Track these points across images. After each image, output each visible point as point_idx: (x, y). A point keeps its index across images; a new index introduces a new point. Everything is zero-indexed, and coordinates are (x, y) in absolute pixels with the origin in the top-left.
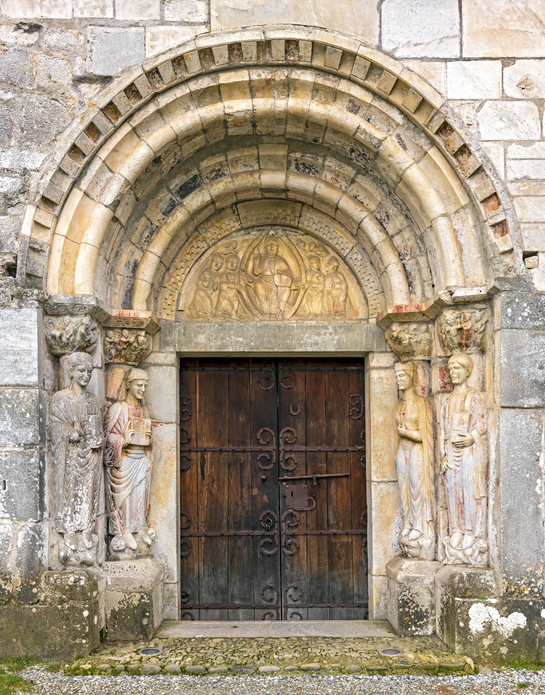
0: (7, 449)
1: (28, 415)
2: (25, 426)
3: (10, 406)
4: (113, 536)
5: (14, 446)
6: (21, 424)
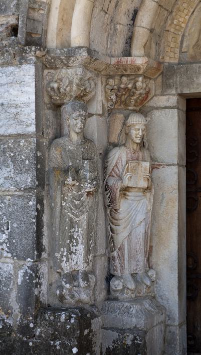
0: (11, 193)
1: (27, 162)
2: (25, 172)
3: (12, 154)
4: (113, 276)
5: (16, 191)
6: (21, 170)
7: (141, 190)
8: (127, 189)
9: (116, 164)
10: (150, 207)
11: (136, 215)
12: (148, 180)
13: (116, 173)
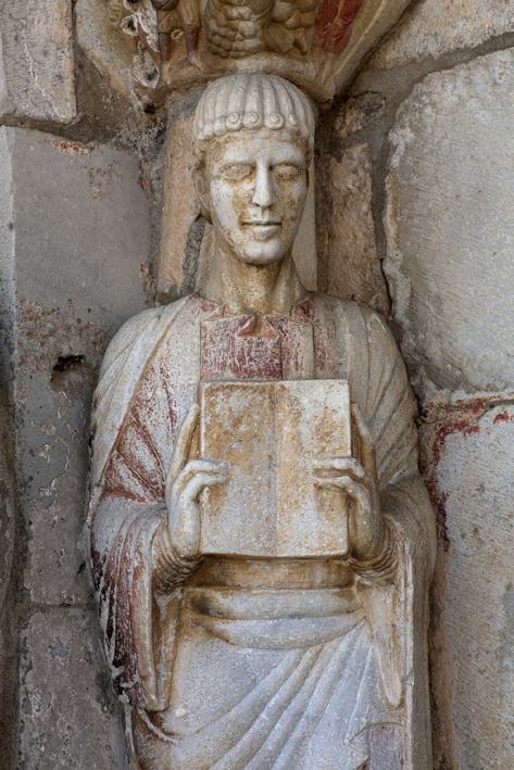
7: (320, 574)
8: (215, 571)
9: (133, 410)
10: (398, 685)
11: (300, 744)
12: (350, 501)
13: (137, 469)
